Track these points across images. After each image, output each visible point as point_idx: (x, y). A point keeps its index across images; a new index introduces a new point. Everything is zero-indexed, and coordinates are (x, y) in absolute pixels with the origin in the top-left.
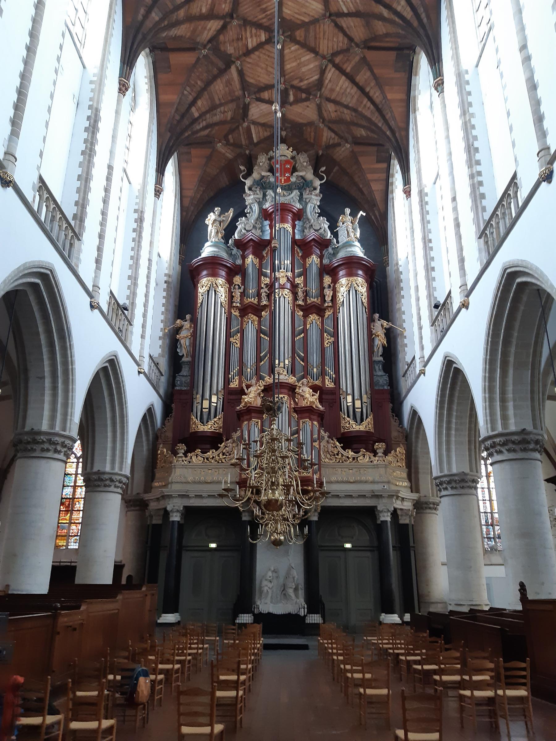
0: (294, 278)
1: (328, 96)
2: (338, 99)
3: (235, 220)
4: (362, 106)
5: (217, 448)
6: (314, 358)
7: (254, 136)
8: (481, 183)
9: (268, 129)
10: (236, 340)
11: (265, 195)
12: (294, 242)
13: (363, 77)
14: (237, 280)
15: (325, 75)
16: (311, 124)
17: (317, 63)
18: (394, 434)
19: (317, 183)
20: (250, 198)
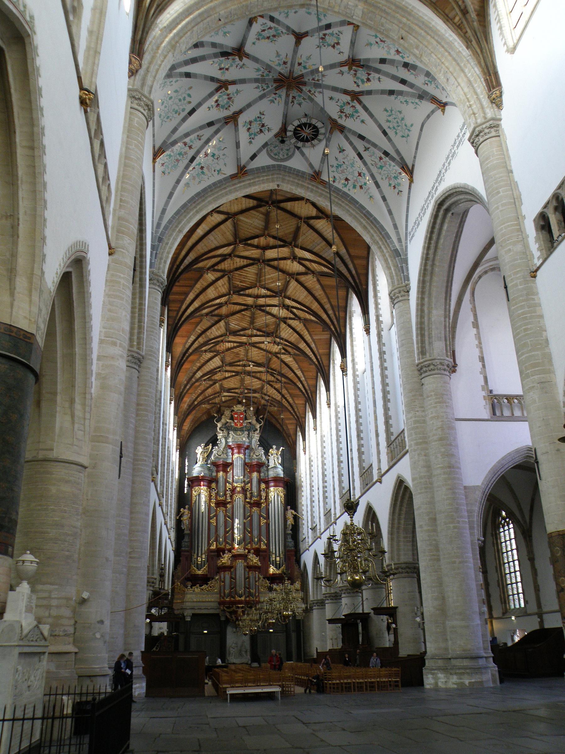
0: (245, 485)
3: (212, 448)
5: (207, 584)
6: (255, 533)
8: (326, 492)
10: (213, 521)
11: (229, 434)
12: (245, 464)
13: (284, 391)
14: (214, 485)
18: (296, 573)
19: (258, 426)
20: (220, 436)
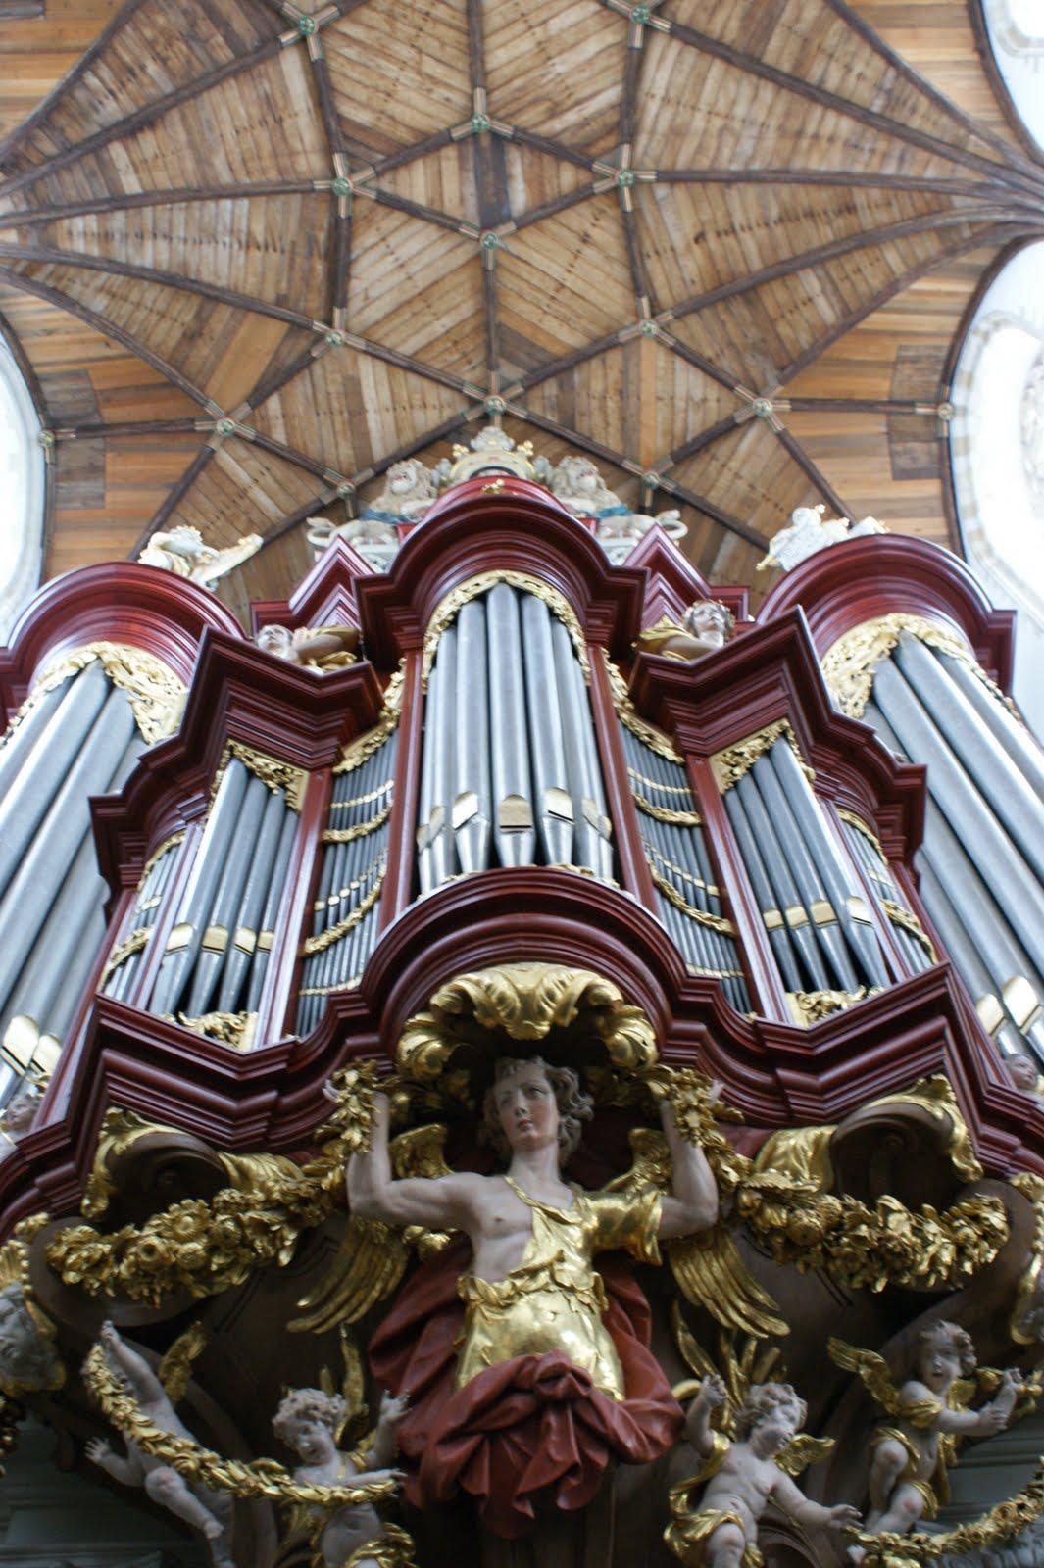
1: (665, 163)
2: (704, 163)
4: (804, 143)
7: (373, 421)
9: (434, 394)
15: (646, 85)
16: (603, 345)
17: (610, 37)
